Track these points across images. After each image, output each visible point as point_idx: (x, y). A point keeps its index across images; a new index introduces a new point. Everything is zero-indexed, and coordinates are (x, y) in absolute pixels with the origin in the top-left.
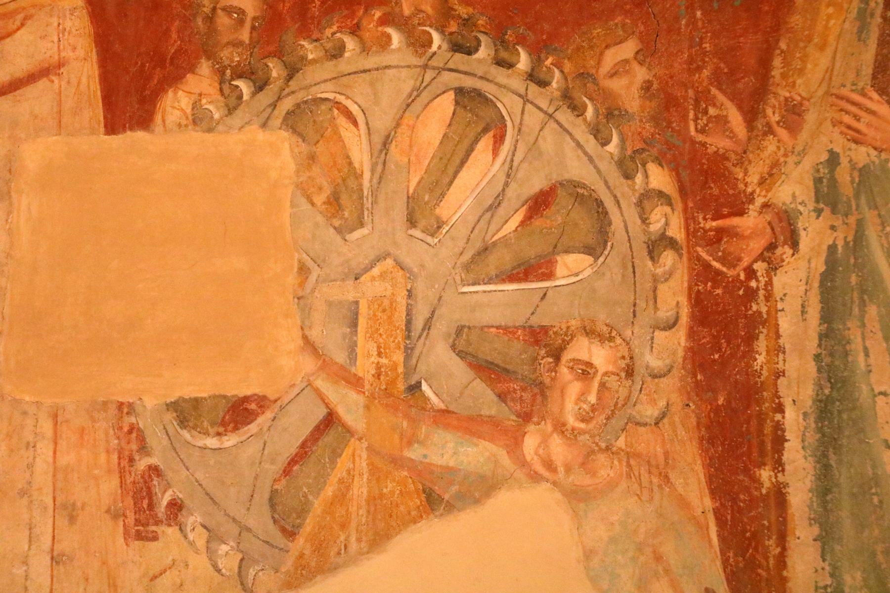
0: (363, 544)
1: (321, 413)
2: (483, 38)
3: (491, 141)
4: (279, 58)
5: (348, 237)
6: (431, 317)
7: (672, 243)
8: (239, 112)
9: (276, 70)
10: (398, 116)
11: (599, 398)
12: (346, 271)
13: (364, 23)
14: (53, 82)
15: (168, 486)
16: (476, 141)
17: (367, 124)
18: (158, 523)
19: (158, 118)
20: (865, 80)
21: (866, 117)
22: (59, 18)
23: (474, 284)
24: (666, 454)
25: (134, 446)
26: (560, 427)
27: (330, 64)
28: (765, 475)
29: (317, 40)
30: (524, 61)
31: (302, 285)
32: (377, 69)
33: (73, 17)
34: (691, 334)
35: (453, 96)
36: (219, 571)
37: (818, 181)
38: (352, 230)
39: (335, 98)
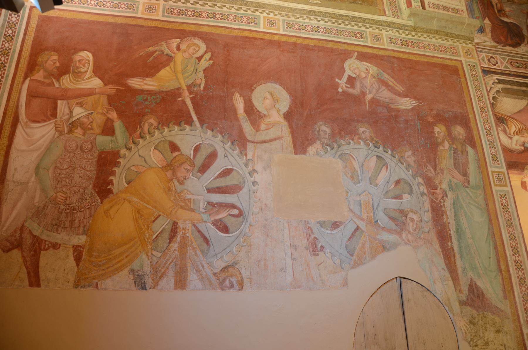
0: (370, 258)
1: (356, 226)
2: (380, 145)
3: (385, 168)
5: (357, 185)
6: (378, 206)
7: (425, 194)
9: (335, 145)
11: (416, 226)
13: (354, 138)
15: (320, 242)
16: (382, 167)
18: (318, 251)
19: (308, 152)
20: (453, 166)
21: (455, 174)
23: (386, 199)
24: (431, 239)
25: (310, 232)
26: (409, 232)
27: (348, 146)
28: (449, 244)
30: (390, 152)
31: (347, 195)
34: (432, 213)
36: (335, 264)
37: (449, 185)
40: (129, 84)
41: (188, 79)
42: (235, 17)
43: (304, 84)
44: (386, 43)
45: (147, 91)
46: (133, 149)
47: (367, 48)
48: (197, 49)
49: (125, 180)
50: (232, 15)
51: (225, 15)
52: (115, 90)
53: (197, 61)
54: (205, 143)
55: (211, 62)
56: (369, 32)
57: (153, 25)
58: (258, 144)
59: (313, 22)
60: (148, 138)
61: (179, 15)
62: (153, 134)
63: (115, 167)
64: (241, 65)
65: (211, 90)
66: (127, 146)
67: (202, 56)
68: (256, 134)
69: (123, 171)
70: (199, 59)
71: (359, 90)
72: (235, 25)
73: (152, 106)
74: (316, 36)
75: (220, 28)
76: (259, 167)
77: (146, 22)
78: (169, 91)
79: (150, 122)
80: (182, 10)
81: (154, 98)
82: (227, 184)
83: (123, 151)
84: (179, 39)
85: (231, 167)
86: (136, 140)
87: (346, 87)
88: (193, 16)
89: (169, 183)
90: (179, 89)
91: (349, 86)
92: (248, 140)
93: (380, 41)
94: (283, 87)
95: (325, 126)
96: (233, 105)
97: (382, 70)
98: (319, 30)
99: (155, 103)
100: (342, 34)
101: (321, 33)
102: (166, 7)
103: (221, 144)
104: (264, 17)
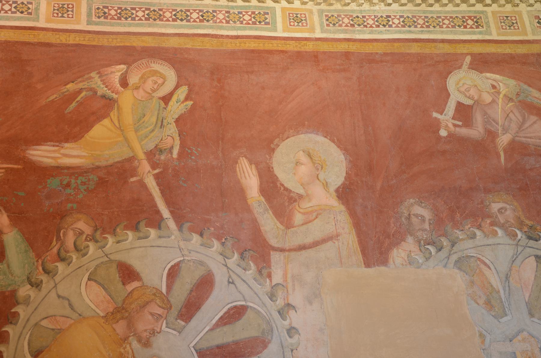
4: (446, 237)
5: (500, 320)
8: (431, 259)
10: (509, 266)
12: (504, 336)
13: (483, 224)
14: (335, 243)
17: (495, 268)
19: (391, 261)
22: (334, 215)
27: (471, 241)
29: (462, 230)
31: (483, 342)
32: (494, 245)
33: (341, 215)
35: (534, 258)
38: (502, 317)
39: (477, 256)
40: (31, 157)
41: (146, 140)
42: (227, 15)
43: (370, 128)
44: (529, 29)
45: (68, 168)
46: (44, 285)
47: (491, 44)
48: (160, 81)
49: (29, 348)
50: (220, 11)
51: (207, 12)
52: (3, 171)
53: (163, 104)
54: (188, 261)
55: (190, 103)
56: (493, 12)
57: (71, 42)
58: (293, 254)
59: (377, 8)
60: (74, 260)
61: (119, 19)
62: (84, 251)
63: (7, 324)
64: (247, 104)
65: (193, 158)
66: (33, 280)
67: (171, 94)
68: (286, 233)
69: (25, 331)
70: (166, 99)
71: (481, 129)
72: (228, 30)
73: (80, 196)
74: (386, 34)
75: (201, 38)
76: (296, 299)
77: (58, 36)
78: (111, 166)
79: (79, 227)
80: (126, 9)
81: (84, 180)
82: (237, 338)
83: (24, 291)
84: (124, 64)
85: (243, 303)
86: (50, 266)
87: (455, 126)
88: (146, 19)
89: (121, 345)
90: (131, 159)
91: (460, 123)
92: (271, 246)
93: (516, 27)
94: (330, 140)
95: (419, 205)
96: (238, 182)
97: (525, 83)
98: (391, 23)
99: (85, 190)
100: (438, 24)
101: (395, 27)
102: (94, 5)
103: (220, 258)
104: (283, 9)
